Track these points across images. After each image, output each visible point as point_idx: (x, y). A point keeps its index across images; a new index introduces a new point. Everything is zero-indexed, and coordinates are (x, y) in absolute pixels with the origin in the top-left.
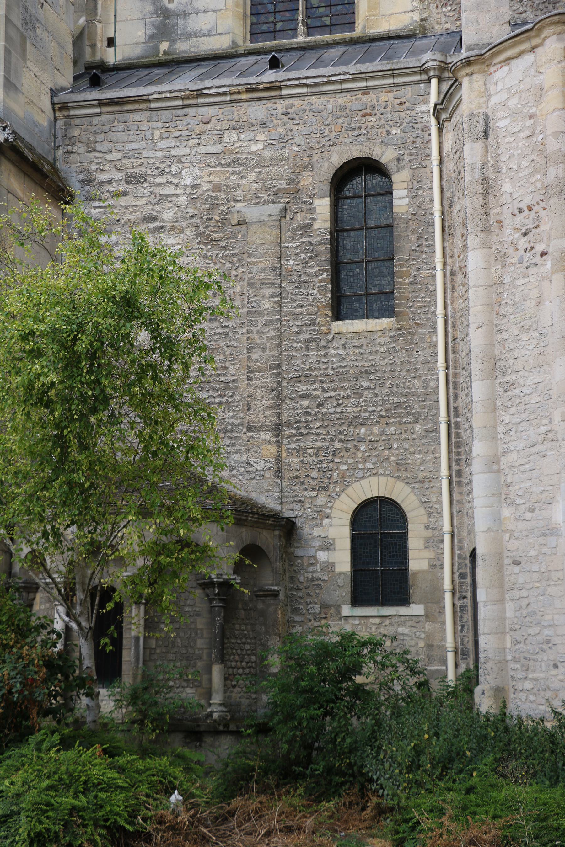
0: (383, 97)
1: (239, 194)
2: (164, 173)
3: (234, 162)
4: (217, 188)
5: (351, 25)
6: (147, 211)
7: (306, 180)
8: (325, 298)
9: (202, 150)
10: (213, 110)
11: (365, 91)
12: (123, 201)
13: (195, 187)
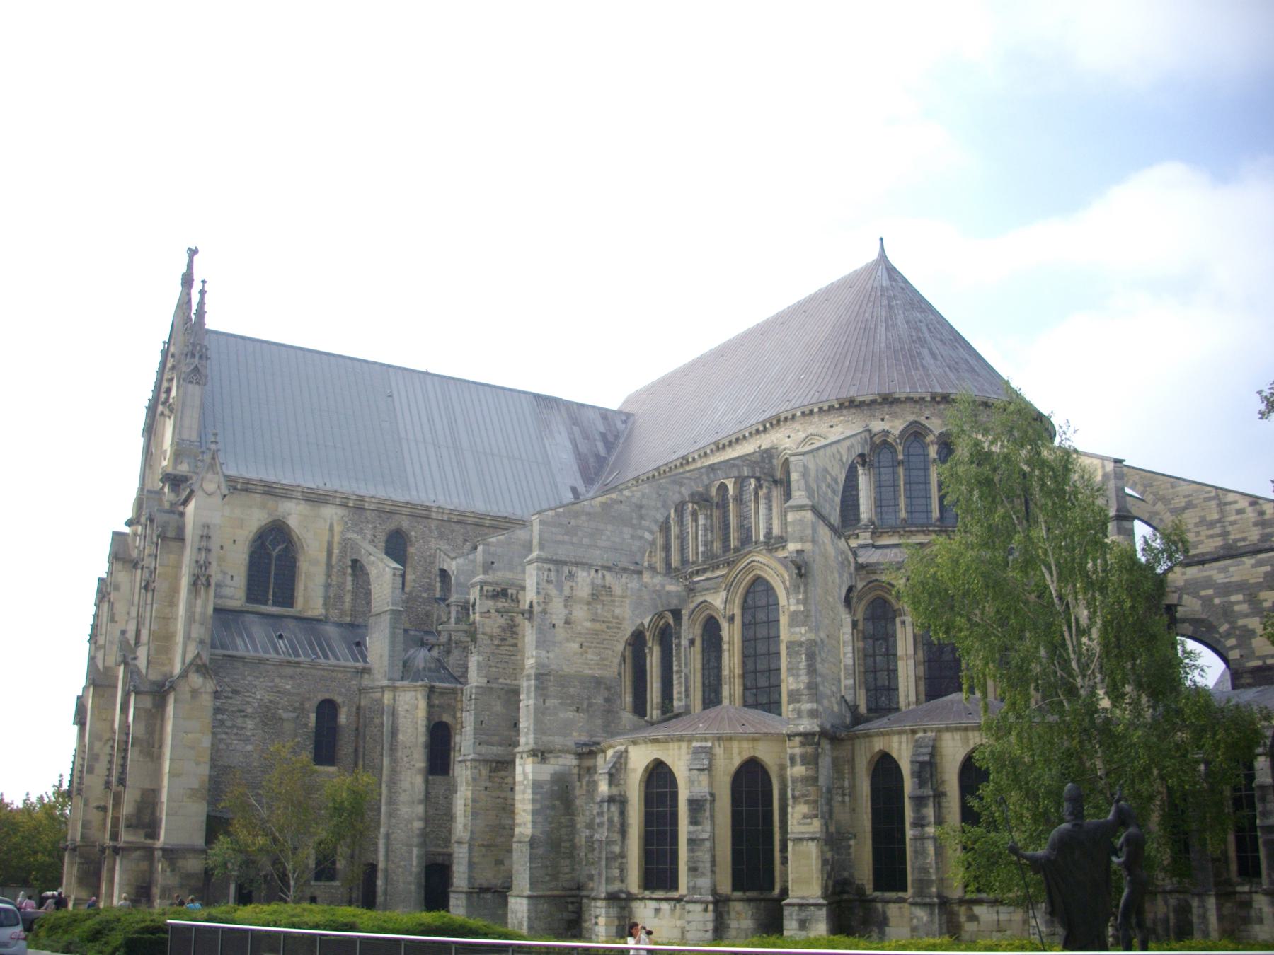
0: (340, 675)
3: (279, 692)
4: (271, 702)
5: (291, 605)
6: (240, 707)
7: (307, 705)
8: (311, 756)
11: (333, 671)
12: (230, 701)
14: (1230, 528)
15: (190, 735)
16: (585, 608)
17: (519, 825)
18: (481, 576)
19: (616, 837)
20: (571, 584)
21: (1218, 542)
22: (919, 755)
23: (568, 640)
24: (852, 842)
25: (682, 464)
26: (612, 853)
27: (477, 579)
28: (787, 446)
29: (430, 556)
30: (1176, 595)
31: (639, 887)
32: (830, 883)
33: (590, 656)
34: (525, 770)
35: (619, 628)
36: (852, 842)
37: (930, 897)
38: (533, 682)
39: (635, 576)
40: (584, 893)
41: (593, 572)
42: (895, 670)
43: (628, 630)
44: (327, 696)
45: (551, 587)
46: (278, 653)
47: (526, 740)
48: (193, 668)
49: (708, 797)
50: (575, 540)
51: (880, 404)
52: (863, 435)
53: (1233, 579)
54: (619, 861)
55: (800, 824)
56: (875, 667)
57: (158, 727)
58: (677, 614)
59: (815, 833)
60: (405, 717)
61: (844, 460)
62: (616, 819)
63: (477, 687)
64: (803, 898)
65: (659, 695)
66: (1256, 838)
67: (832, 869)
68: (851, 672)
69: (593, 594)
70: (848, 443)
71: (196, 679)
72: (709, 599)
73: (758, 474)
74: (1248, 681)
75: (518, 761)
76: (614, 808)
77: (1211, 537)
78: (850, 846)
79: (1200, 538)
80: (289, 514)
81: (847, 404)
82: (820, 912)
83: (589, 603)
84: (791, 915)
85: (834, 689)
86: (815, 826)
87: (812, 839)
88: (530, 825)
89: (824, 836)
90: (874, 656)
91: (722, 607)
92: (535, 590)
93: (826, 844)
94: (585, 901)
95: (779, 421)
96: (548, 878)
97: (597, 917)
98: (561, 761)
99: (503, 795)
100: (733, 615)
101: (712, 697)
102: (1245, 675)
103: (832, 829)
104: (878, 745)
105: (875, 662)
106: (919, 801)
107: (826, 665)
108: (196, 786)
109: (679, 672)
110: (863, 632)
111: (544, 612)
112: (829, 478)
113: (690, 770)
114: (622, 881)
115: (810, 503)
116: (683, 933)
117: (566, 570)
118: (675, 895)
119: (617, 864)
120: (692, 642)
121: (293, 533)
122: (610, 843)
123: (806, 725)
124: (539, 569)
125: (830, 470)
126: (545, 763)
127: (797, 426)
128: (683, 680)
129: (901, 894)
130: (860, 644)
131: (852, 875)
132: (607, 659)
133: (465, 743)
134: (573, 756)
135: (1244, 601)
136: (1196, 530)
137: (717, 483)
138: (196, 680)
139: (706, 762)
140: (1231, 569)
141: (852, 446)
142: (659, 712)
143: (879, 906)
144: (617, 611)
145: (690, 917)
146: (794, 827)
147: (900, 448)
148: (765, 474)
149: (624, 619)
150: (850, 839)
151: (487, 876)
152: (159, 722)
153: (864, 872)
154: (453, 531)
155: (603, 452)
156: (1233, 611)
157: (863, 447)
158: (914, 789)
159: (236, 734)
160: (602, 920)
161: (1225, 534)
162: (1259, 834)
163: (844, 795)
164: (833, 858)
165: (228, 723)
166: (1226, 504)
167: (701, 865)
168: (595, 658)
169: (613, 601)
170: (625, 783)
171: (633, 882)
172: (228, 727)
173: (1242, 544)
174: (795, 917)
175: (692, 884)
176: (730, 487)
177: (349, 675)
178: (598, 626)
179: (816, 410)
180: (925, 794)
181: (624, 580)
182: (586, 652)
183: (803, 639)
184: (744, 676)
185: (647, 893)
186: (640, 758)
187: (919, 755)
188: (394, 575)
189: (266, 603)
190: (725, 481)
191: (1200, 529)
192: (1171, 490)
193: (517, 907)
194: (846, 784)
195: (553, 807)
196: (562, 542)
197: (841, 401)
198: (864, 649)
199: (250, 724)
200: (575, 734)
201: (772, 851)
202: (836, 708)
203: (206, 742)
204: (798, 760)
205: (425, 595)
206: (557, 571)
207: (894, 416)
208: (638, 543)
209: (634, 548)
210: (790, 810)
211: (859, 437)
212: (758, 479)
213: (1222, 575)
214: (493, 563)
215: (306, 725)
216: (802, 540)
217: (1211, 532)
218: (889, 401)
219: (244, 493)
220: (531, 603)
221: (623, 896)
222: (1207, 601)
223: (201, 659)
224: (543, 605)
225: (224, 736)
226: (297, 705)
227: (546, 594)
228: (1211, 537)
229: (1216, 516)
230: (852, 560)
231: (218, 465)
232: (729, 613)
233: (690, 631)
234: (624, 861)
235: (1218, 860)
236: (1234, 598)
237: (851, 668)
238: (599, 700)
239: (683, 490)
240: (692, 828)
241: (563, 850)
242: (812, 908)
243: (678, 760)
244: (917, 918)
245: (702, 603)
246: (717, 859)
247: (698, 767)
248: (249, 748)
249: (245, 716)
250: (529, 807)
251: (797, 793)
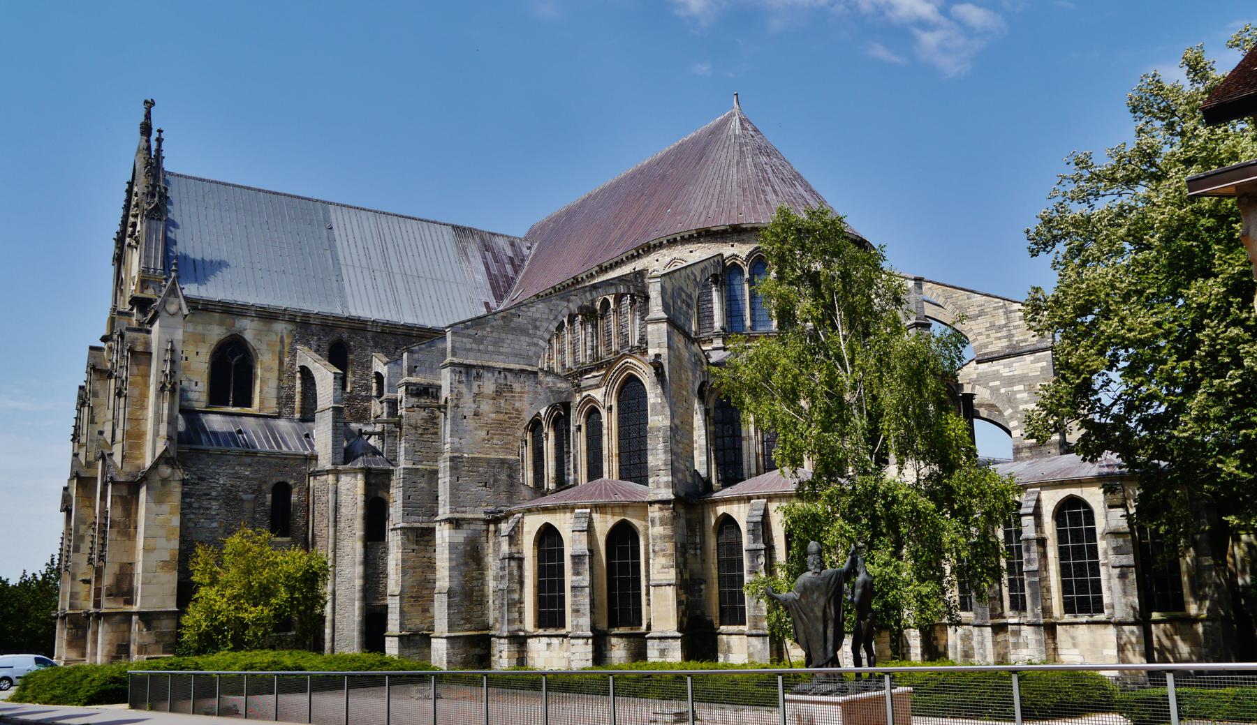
1: (240, 489)
2: (212, 478)
3: (239, 478)
4: (232, 486)
6: (206, 491)
7: (264, 487)
9: (227, 471)
10: (231, 457)
12: (197, 487)
13: (224, 484)
14: (1014, 332)
15: (161, 517)
16: (491, 402)
17: (439, 579)
18: (407, 378)
19: (517, 587)
20: (479, 383)
21: (1005, 343)
22: (753, 516)
23: (476, 429)
24: (703, 587)
25: (572, 283)
26: (512, 600)
27: (402, 381)
28: (656, 268)
29: (367, 361)
30: (970, 386)
31: (535, 626)
32: (685, 620)
33: (495, 442)
34: (443, 535)
35: (519, 418)
36: (703, 587)
37: (763, 629)
38: (448, 463)
39: (531, 376)
40: (492, 633)
41: (496, 374)
42: (740, 449)
43: (527, 417)
44: (281, 479)
45: (463, 385)
46: (238, 446)
47: (444, 511)
48: (163, 461)
49: (588, 553)
50: (481, 347)
51: (730, 233)
52: (716, 259)
53: (1016, 373)
54: (518, 605)
55: (658, 573)
56: (724, 446)
57: (133, 510)
58: (566, 406)
59: (672, 579)
60: (347, 495)
61: (698, 280)
62: (515, 572)
63: (404, 469)
64: (662, 632)
65: (554, 471)
66: (1022, 581)
67: (686, 609)
68: (705, 450)
69: (497, 391)
70: (702, 265)
71: (165, 470)
72: (592, 393)
73: (632, 292)
74: (1027, 455)
75: (438, 528)
76: (513, 563)
77: (999, 338)
78: (702, 590)
79: (990, 340)
80: (245, 329)
81: (703, 233)
82: (676, 643)
83: (494, 399)
84: (653, 646)
85: (688, 464)
86: (671, 575)
87: (669, 585)
88: (447, 579)
89: (679, 582)
90: (723, 437)
91: (603, 398)
92: (449, 389)
93: (681, 589)
94: (493, 639)
95: (649, 248)
96: (462, 622)
97: (501, 652)
98: (472, 527)
99: (428, 555)
100: (611, 406)
101: (595, 471)
102: (1024, 450)
103: (686, 576)
104: (721, 510)
105: (724, 442)
106: (754, 553)
107: (681, 446)
108: (168, 559)
109: (568, 452)
110: (714, 418)
111: (457, 406)
112: (684, 296)
113: (573, 531)
114: (521, 622)
115: (666, 316)
116: (569, 662)
117: (474, 372)
118: (563, 632)
119: (517, 609)
120: (579, 428)
121: (249, 346)
122: (510, 591)
123: (667, 494)
124: (452, 371)
125: (685, 288)
126: (459, 529)
127: (664, 251)
128: (572, 459)
129: (741, 627)
130: (712, 428)
131: (703, 613)
132: (509, 443)
133: (396, 514)
134: (482, 523)
135: (1025, 390)
136: (987, 333)
137: (601, 299)
138: (166, 471)
139: (586, 525)
140: (1014, 365)
141: (706, 268)
142: (554, 485)
143: (725, 637)
144: (517, 405)
145: (573, 649)
146: (656, 576)
147: (746, 269)
148: (638, 291)
149: (522, 410)
150: (702, 584)
151: (416, 622)
152: (134, 507)
153: (714, 611)
154: (386, 341)
155: (510, 273)
156: (1015, 399)
157: (716, 269)
158: (749, 543)
159: (204, 514)
160: (505, 654)
161: (1010, 337)
162: (1025, 577)
163: (696, 549)
164: (687, 599)
165: (196, 505)
166: (1011, 312)
167: (582, 607)
168: (499, 443)
169: (513, 396)
170: (522, 543)
171: (529, 623)
172: (195, 508)
173: (1024, 344)
174: (656, 647)
175: (575, 623)
176: (611, 301)
177: (299, 461)
178: (501, 416)
179: (679, 238)
180: (758, 548)
181: (522, 379)
182: (493, 438)
183: (660, 425)
184: (619, 455)
185: (541, 632)
186: (532, 524)
187: (753, 516)
188: (335, 378)
189: (227, 405)
190: (607, 297)
191: (990, 332)
192: (967, 301)
193: (439, 646)
194: (698, 540)
195: (466, 564)
196: (471, 350)
197: (699, 231)
198: (715, 432)
199: (215, 505)
200: (484, 504)
201: (639, 595)
202: (689, 480)
203: (176, 521)
204: (657, 521)
205: (363, 394)
206: (467, 373)
207: (743, 242)
208: (533, 349)
209: (531, 353)
210: (651, 561)
211: (712, 261)
212: (632, 296)
213: (1007, 370)
214: (416, 367)
215: (263, 504)
216: (659, 345)
217: (999, 335)
218: (736, 233)
219: (205, 312)
220: (446, 398)
221: (522, 634)
222: (994, 390)
223: (169, 453)
224: (455, 401)
225: (192, 516)
226: (256, 487)
227: (459, 392)
228: (999, 338)
229: (1003, 322)
230: (704, 361)
231: (179, 290)
232: (607, 405)
233: (577, 419)
234: (522, 605)
235: (994, 598)
236: (1016, 388)
237: (705, 447)
238: (503, 477)
239: (571, 305)
240: (575, 578)
241: (475, 598)
242: (670, 640)
243: (564, 523)
244: (753, 646)
245: (586, 396)
246: (596, 602)
247: (578, 529)
248: (215, 525)
249: (210, 499)
250: (447, 564)
251: (657, 548)
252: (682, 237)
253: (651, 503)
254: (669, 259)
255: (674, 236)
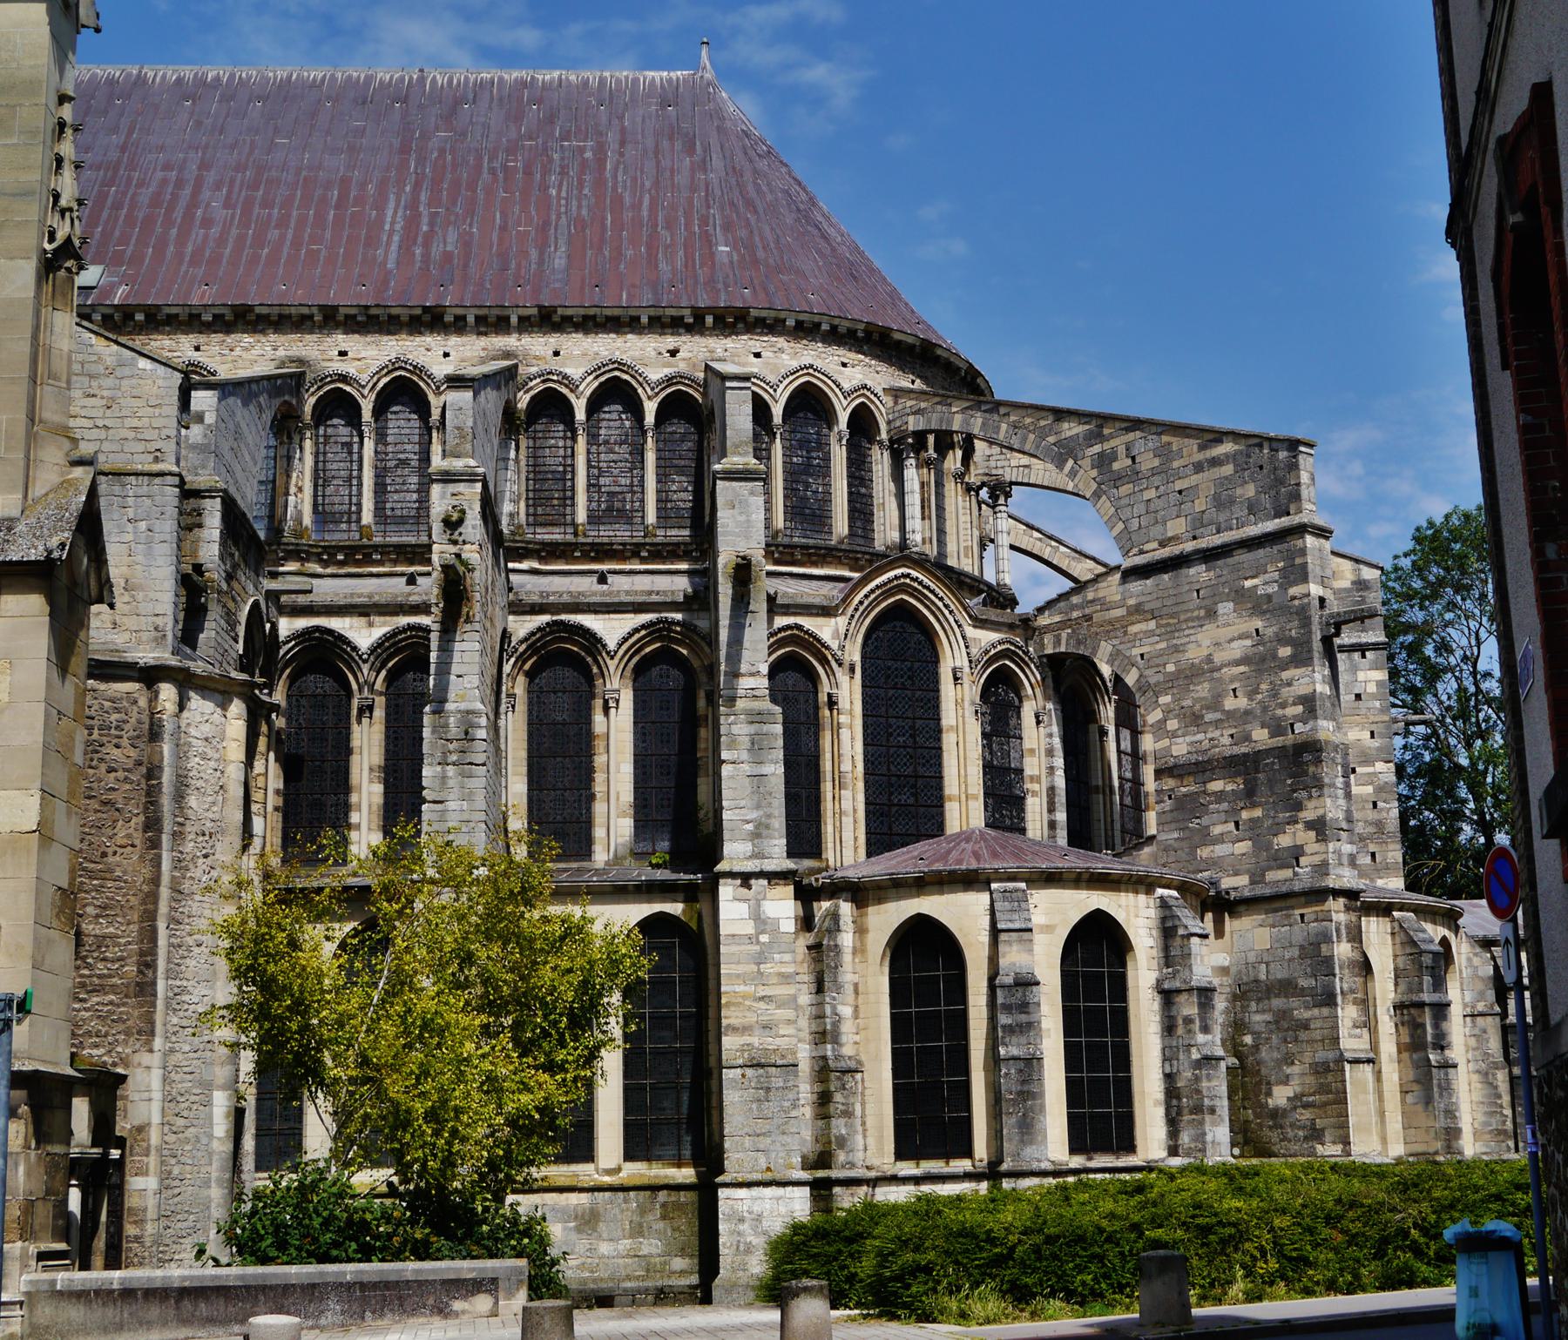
55: (1351, 1036)
81: (876, 336)
127: (781, 342)
167: (1217, 1102)
197: (871, 328)
245: (788, 627)
251: (1345, 986)
252: (834, 328)
253: (1337, 893)
254: (795, 364)
255: (816, 319)
